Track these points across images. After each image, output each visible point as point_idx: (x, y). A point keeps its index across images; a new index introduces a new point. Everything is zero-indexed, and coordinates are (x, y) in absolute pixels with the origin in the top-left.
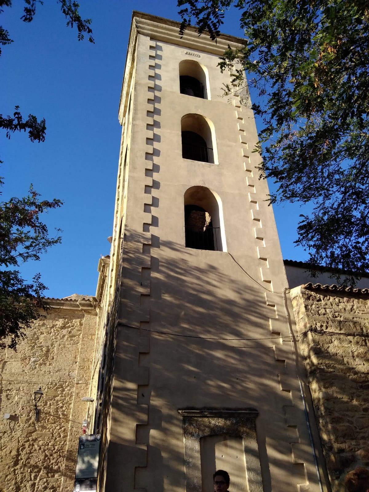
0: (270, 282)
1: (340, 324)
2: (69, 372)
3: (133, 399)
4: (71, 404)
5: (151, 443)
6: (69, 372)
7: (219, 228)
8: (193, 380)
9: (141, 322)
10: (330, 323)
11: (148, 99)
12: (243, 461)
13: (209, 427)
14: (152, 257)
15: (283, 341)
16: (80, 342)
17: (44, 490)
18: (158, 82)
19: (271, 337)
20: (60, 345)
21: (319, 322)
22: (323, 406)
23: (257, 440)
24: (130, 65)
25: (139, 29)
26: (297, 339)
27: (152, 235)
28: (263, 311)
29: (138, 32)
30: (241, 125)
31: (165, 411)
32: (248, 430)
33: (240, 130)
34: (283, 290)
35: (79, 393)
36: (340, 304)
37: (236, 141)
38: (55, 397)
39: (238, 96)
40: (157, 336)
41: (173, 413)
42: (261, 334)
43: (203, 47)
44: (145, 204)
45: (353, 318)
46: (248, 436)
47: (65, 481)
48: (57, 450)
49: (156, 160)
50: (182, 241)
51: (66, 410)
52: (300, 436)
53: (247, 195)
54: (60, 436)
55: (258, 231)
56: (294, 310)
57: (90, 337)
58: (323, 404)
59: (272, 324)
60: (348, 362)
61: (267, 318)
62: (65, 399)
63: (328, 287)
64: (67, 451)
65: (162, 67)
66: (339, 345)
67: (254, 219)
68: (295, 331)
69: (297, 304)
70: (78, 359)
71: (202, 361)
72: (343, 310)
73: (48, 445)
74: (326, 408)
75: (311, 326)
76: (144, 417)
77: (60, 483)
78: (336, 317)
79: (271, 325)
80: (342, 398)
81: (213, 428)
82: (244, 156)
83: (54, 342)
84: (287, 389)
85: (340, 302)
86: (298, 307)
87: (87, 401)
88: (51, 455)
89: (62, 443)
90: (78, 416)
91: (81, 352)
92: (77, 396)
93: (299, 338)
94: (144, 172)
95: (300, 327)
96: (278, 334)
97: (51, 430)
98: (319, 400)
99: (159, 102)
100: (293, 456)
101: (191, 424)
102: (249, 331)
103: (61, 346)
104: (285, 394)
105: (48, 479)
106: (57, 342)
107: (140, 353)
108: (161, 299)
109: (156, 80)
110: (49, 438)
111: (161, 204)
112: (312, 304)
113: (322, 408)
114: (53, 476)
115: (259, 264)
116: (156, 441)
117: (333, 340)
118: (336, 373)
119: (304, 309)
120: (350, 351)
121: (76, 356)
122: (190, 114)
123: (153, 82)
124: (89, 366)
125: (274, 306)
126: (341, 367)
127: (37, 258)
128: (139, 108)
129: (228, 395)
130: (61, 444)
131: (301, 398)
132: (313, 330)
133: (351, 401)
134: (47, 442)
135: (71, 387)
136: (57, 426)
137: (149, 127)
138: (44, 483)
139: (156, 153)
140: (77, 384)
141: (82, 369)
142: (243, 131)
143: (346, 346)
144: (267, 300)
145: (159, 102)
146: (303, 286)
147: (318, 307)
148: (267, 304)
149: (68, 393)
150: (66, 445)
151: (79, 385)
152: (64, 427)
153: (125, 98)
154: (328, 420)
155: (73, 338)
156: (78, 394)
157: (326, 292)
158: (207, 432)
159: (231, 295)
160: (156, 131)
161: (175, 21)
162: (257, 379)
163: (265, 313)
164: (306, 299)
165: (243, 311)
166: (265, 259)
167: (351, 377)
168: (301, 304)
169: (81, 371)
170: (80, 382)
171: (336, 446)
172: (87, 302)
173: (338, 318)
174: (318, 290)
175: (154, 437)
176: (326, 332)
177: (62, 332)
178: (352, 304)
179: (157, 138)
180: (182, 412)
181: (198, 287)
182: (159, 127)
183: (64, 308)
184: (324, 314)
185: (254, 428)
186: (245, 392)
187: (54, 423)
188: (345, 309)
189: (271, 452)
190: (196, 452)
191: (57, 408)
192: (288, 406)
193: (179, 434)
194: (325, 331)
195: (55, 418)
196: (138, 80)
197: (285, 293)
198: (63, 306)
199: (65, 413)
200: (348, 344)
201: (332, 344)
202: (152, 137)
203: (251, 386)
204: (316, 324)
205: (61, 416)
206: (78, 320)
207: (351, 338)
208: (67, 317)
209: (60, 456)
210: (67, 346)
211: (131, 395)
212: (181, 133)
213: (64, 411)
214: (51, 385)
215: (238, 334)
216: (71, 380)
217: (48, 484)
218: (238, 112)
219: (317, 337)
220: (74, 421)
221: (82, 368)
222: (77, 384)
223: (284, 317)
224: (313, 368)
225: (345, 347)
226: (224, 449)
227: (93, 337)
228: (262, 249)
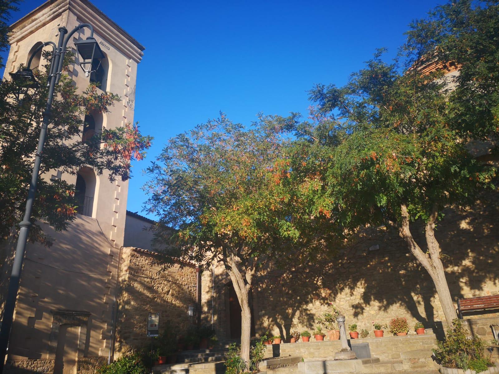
55: (116, 207)
146: (132, 248)
166: (116, 226)
174: (139, 252)
228: (115, 219)
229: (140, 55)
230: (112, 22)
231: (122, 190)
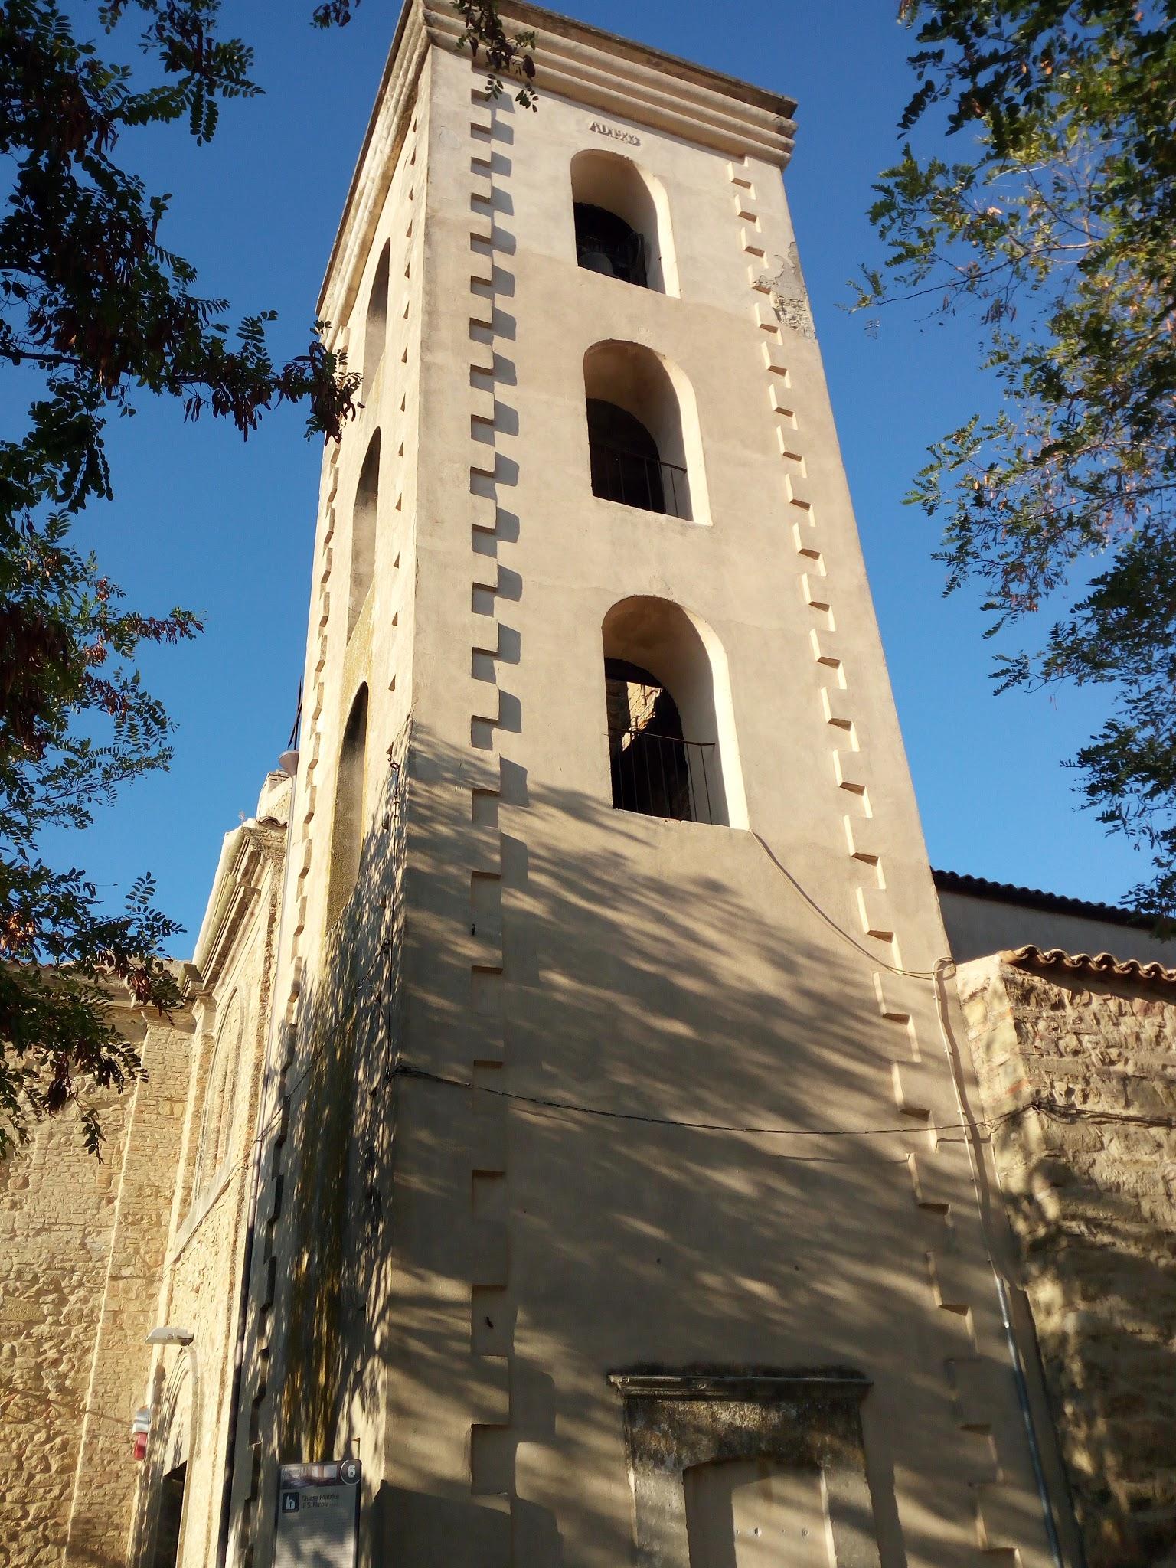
0: (887, 937)
1: (1125, 1086)
2: (84, 1236)
3: (459, 1337)
4: (88, 1350)
5: (521, 1492)
6: (84, 1236)
7: (714, 745)
8: (651, 1272)
9: (478, 1064)
10: (1095, 1079)
11: (474, 279)
12: (821, 1545)
13: (712, 1433)
14: (504, 838)
15: (940, 1140)
16: (130, 1127)
18: (501, 220)
19: (898, 1126)
20: (51, 1136)
21: (1061, 1080)
22: (1077, 1358)
23: (867, 1475)
24: (387, 150)
25: (436, 31)
26: (983, 1135)
27: (503, 762)
28: (872, 1037)
29: (432, 40)
30: (781, 393)
31: (565, 1379)
32: (837, 1443)
33: (779, 410)
34: (933, 968)
35: (121, 1311)
36: (1122, 1019)
37: (766, 447)
38: (31, 1323)
39: (767, 291)
40: (529, 1115)
41: (592, 1385)
42: (869, 1115)
43: (650, 110)
44: (475, 651)
45: (1164, 1067)
46: (840, 1462)
48: (35, 1518)
49: (506, 496)
50: (600, 786)
52: (1000, 1460)
53: (806, 638)
54: (47, 1468)
55: (847, 760)
56: (972, 1034)
57: (165, 1109)
58: (1080, 1352)
59: (903, 1081)
60: (1153, 1214)
61: (883, 1063)
62: (68, 1333)
63: (1085, 960)
64: (75, 1521)
65: (514, 168)
66: (1126, 1157)
67: (833, 722)
68: (975, 1107)
69: (985, 1017)
70: (120, 1190)
71: (681, 1207)
72: (1131, 1040)
74: (1089, 1367)
75: (1038, 1092)
76: (497, 1399)
78: (1112, 1063)
79: (899, 1085)
80: (1140, 1332)
81: (726, 1435)
82: (794, 502)
84: (956, 1304)
85: (1121, 1014)
86: (989, 1026)
87: (169, 1340)
88: (14, 1537)
90: (117, 1396)
91: (130, 1161)
92: (115, 1321)
93: (989, 1131)
94: (470, 536)
95: (994, 1093)
96: (922, 1115)
97: (14, 1446)
98: (1063, 1338)
99: (510, 292)
100: (980, 1525)
101: (652, 1424)
102: (829, 1103)
104: (950, 1318)
107: (478, 1174)
108: (536, 982)
109: (497, 213)
111: (527, 650)
112: (1038, 1018)
113: (1076, 1367)
115: (853, 876)
116: (540, 1483)
117: (1106, 1140)
118: (1121, 1246)
119: (1014, 1033)
120: (1158, 1177)
121: (111, 1176)
122: (612, 341)
123: (486, 219)
124: (159, 1216)
125: (903, 1019)
126: (1133, 1228)
127: (82, 818)
128: (442, 307)
129: (769, 1321)
130: (48, 1496)
131: (1002, 1335)
132: (1044, 1105)
133: (1166, 1342)
135: (90, 1291)
136: (38, 1431)
137: (480, 376)
139: (506, 471)
140: (115, 1278)
142: (789, 414)
143: (1146, 1158)
144: (885, 1000)
145: (510, 292)
147: (1055, 1029)
148: (884, 1009)
149: (81, 1310)
150: (69, 1499)
151: (121, 1283)
153: (353, 261)
154: (1096, 1404)
156: (116, 1314)
157: (1080, 978)
158: (705, 1450)
159: (764, 978)
160: (503, 392)
161: (557, 14)
162: (859, 1270)
163: (876, 1044)
164: (1017, 1000)
165: (807, 1034)
166: (871, 860)
167: (1162, 1262)
168: (1002, 1016)
169: (129, 1234)
170: (125, 1272)
171: (1121, 1490)
173: (1119, 1067)
174: (1054, 971)
175: (529, 1470)
176: (1084, 1112)
178: (1159, 1019)
179: (503, 420)
180: (623, 1383)
181: (657, 949)
182: (512, 380)
184: (1076, 1053)
185: (856, 1436)
186: (823, 1310)
187: (28, 1419)
188: (1138, 1038)
189: (912, 1516)
190: (674, 1517)
191: (39, 1366)
192: (956, 1359)
193: (613, 1458)
194: (1079, 1107)
195: (32, 1401)
196: (436, 206)
197: (940, 978)
199: (68, 1382)
200: (1151, 1154)
201: (1103, 1154)
202: (490, 415)
203: (839, 1290)
204: (1053, 1087)
207: (1157, 1132)
209: (46, 1541)
211: (451, 1320)
212: (584, 409)
213: (64, 1376)
214: (17, 1279)
215: (796, 1114)
216: (91, 1264)
218: (768, 344)
219: (1057, 1129)
220: (98, 1414)
221: (131, 1219)
222: (115, 1278)
223: (940, 1060)
224: (1042, 1231)
225: (1144, 1164)
226: (760, 1507)
227: (177, 1107)
228: (861, 825)
229: (781, 130)
230: (622, 43)
231: (852, 677)
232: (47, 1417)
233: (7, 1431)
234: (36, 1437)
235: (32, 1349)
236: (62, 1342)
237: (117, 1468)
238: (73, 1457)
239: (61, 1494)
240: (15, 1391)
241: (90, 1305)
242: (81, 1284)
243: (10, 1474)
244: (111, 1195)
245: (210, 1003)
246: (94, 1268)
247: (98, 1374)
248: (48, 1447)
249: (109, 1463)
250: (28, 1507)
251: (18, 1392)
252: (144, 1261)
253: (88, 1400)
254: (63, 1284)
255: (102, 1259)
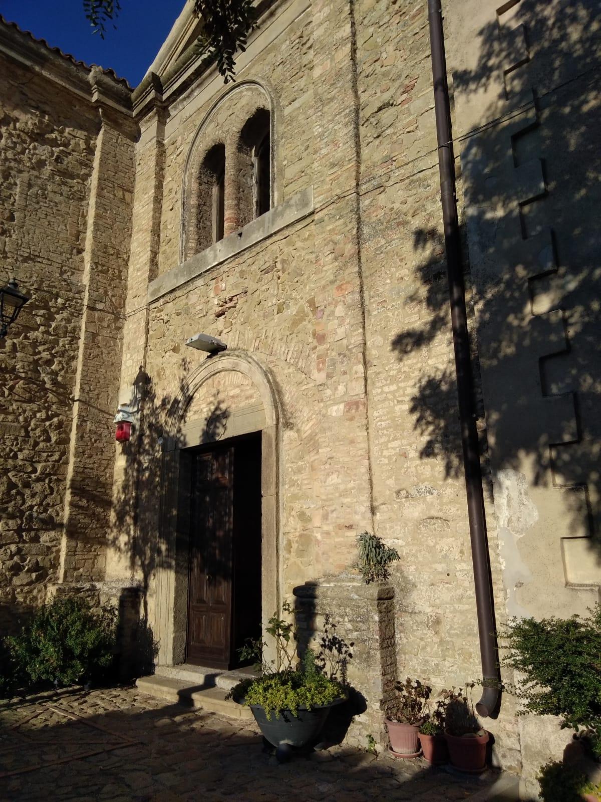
4: (74, 358)
17: (13, 575)
20: (30, 186)
35: (97, 334)
47: (71, 553)
48: (42, 473)
51: (62, 373)
54: (48, 439)
73: (15, 457)
77: (57, 558)
83: (10, 168)
88: (27, 485)
89: (56, 457)
90: (98, 395)
92: (93, 341)
97: (21, 419)
103: (34, 190)
105: (20, 545)
106: (20, 172)
110: (16, 439)
114: (36, 539)
124: (120, 272)
134: (11, 450)
135: (72, 314)
136: (39, 411)
138: (12, 557)
141: (101, 272)
149: (66, 327)
150: (67, 463)
151: (97, 314)
152: (57, 415)
155: (69, 180)
170: (100, 306)
172: (120, 86)
177: (35, 148)
183: (45, 73)
187: (30, 401)
191: (36, 362)
198: (42, 66)
199: (60, 379)
205: (48, 386)
206: (81, 134)
208: (47, 108)
210: (51, 195)
213: (57, 374)
216: (71, 295)
217: (23, 560)
227: (127, 195)
232: (46, 402)
233: (14, 407)
234: (38, 415)
235: (29, 348)
236: (53, 348)
237: (101, 445)
238: (67, 433)
239: (60, 459)
240: (18, 377)
241: (72, 324)
242: (64, 307)
243: (20, 439)
244: (80, 247)
245: (164, 116)
246: (74, 298)
247: (84, 377)
248: (48, 423)
249: (96, 441)
250: (35, 465)
251: (21, 378)
252: (111, 301)
253: (77, 394)
254: (50, 304)
255: (79, 292)
